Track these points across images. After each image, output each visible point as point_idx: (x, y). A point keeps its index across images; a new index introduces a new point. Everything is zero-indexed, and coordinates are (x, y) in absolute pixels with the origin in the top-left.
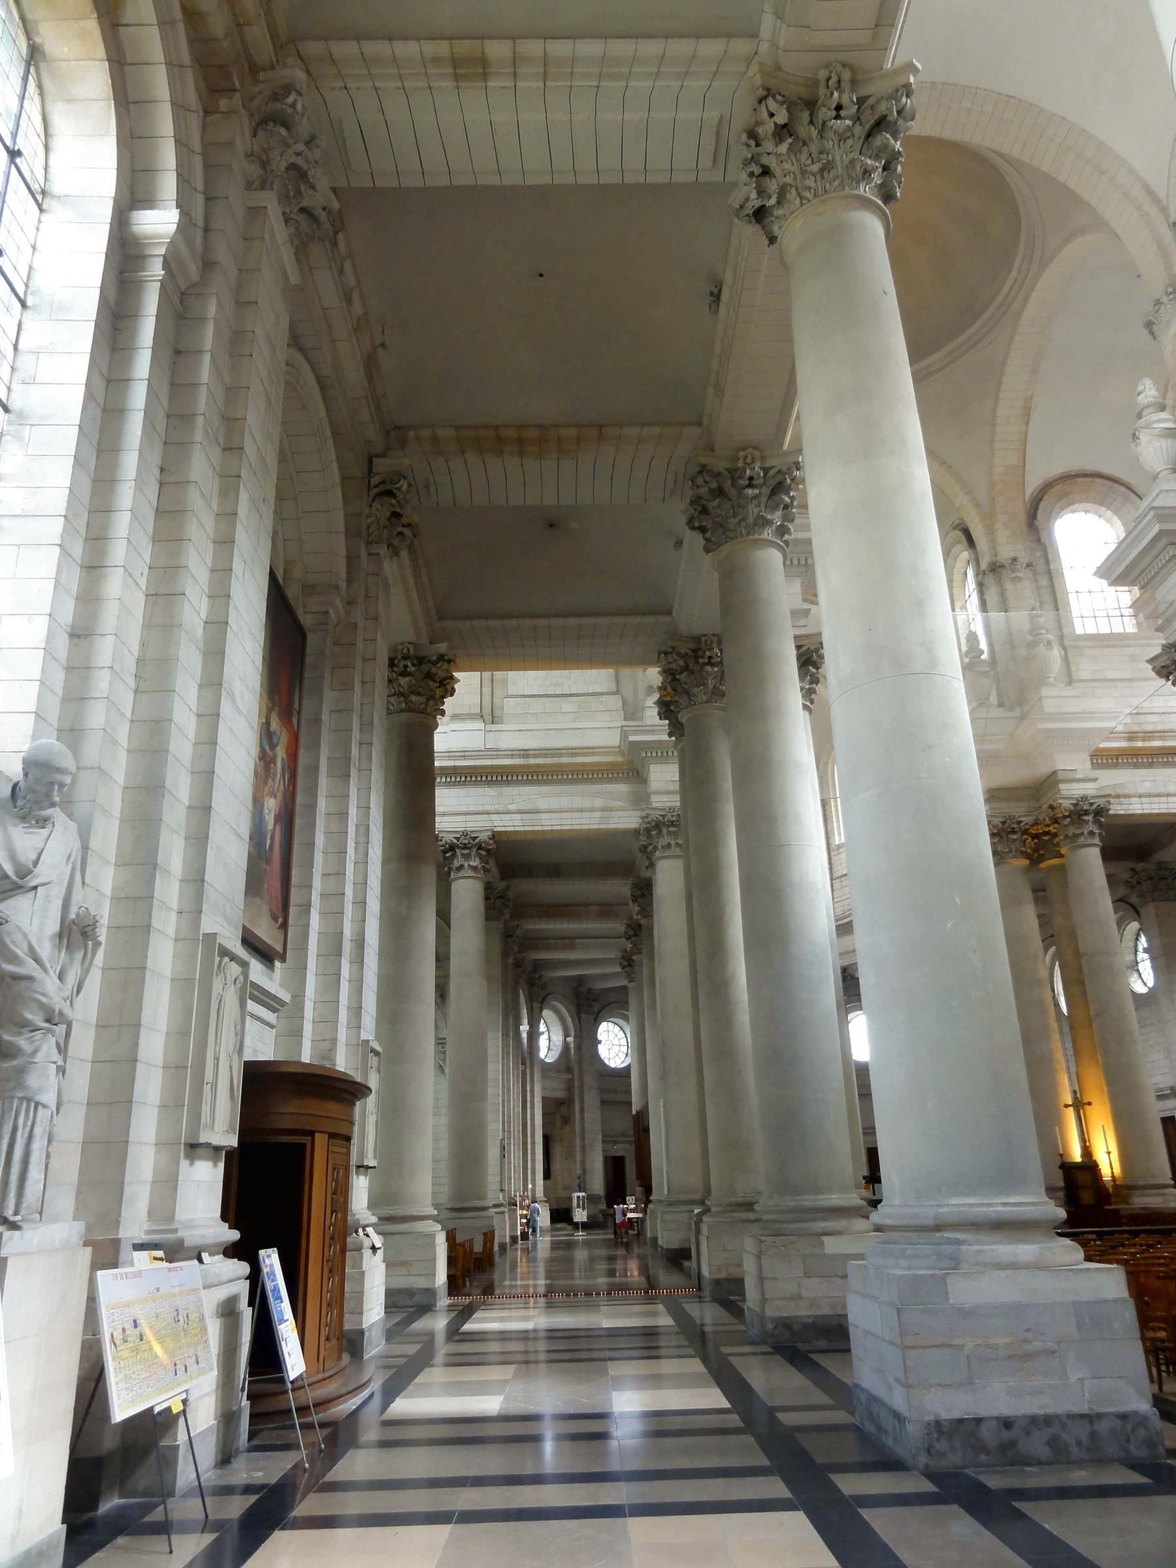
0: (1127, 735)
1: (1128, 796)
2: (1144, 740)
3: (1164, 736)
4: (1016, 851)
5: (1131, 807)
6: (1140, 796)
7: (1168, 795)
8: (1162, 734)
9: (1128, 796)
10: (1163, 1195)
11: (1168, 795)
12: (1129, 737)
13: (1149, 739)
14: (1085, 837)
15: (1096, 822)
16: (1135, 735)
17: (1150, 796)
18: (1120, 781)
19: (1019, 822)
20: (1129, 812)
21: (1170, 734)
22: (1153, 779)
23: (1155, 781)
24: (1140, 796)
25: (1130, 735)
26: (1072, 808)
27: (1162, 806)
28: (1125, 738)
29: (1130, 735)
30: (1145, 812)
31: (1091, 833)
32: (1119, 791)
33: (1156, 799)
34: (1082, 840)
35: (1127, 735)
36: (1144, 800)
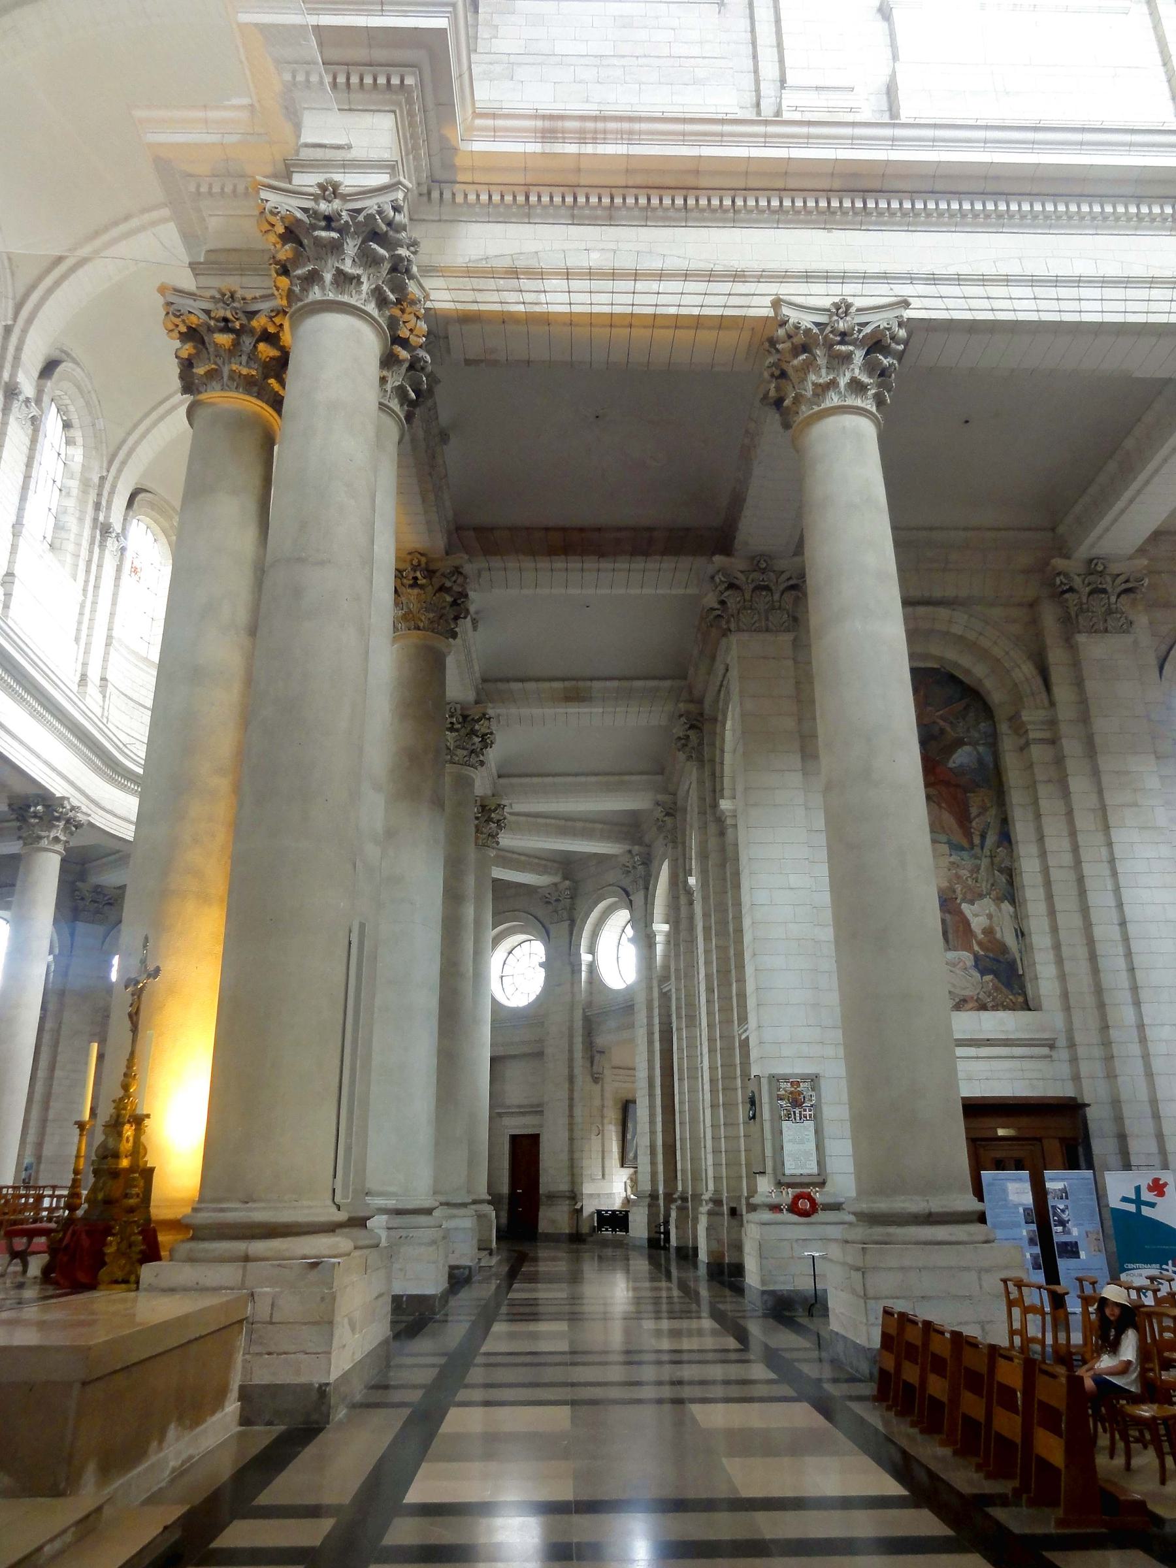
0: (539, 123)
1: (541, 275)
2: (582, 137)
3: (631, 132)
4: (231, 378)
5: (542, 298)
6: (568, 275)
7: (636, 276)
8: (626, 126)
9: (541, 275)
10: (246, 1259)
11: (636, 276)
12: (544, 131)
13: (596, 137)
14: (323, 288)
15: (368, 259)
16: (559, 124)
17: (591, 274)
18: (530, 247)
19: (252, 314)
20: (537, 309)
21: (644, 126)
22: (612, 246)
23: (615, 251)
24: (568, 275)
25: (547, 124)
26: (299, 215)
27: (619, 299)
28: (535, 131)
29: (547, 124)
30: (576, 309)
31: (344, 280)
32: (521, 263)
33: (608, 285)
34: (316, 294)
35: (539, 123)
36: (576, 284)
